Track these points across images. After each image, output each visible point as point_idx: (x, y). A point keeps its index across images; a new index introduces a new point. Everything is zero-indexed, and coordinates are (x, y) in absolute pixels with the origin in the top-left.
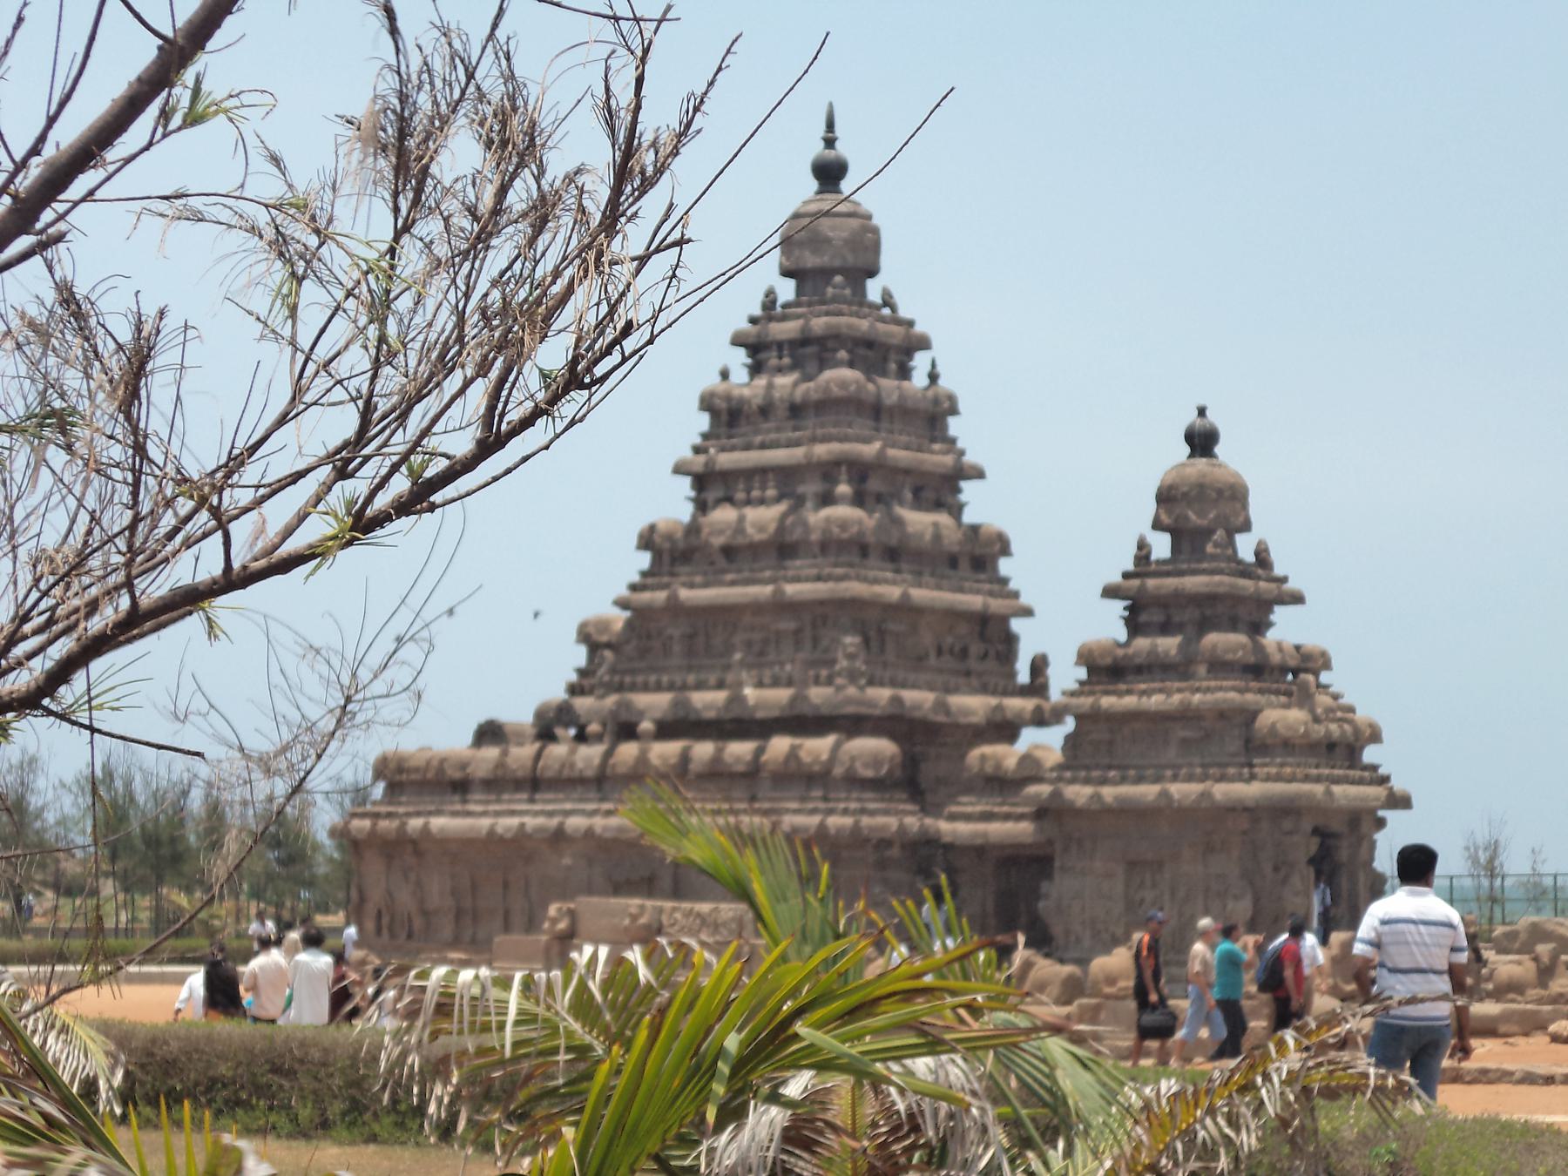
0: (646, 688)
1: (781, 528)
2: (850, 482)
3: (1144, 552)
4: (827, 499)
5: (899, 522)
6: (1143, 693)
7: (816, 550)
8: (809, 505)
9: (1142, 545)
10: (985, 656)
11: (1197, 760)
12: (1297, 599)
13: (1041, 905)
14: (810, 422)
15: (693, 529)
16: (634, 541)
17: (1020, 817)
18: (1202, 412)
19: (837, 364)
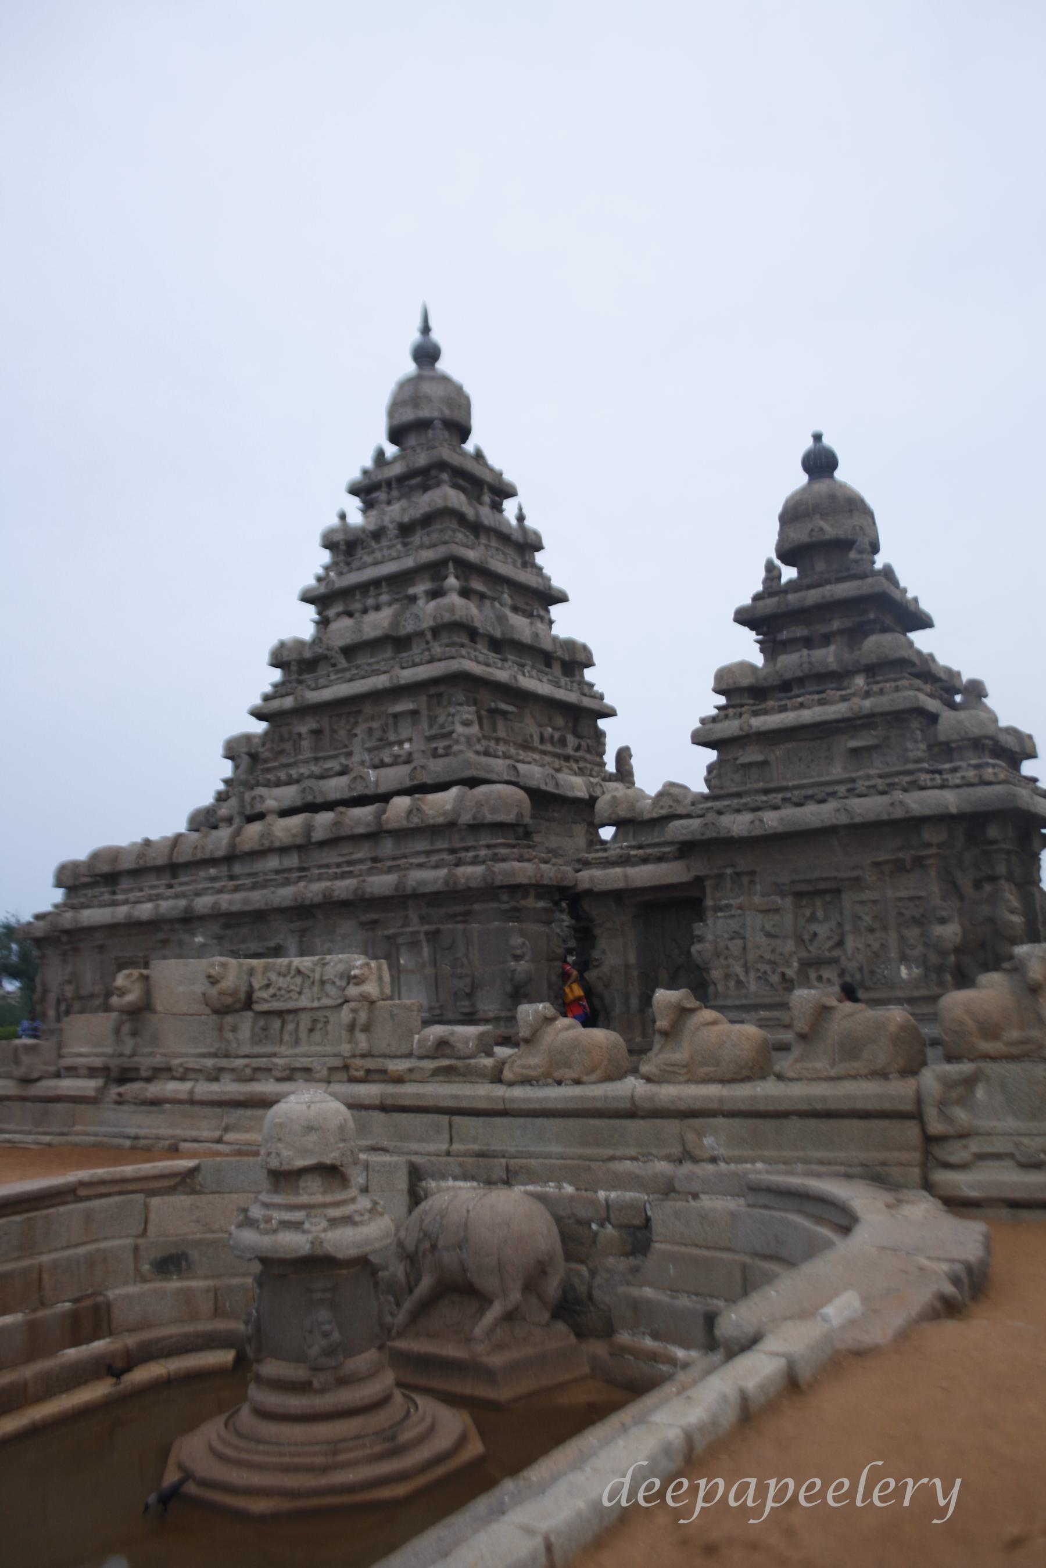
0: (278, 784)
1: (395, 623)
2: (457, 577)
3: (775, 573)
4: (435, 594)
5: (501, 619)
6: (802, 706)
7: (429, 636)
8: (421, 602)
9: (770, 567)
10: (578, 749)
11: (873, 772)
12: (923, 622)
13: (695, 949)
14: (416, 539)
15: (317, 641)
16: (266, 658)
17: (661, 859)
18: (817, 438)
19: (438, 484)
